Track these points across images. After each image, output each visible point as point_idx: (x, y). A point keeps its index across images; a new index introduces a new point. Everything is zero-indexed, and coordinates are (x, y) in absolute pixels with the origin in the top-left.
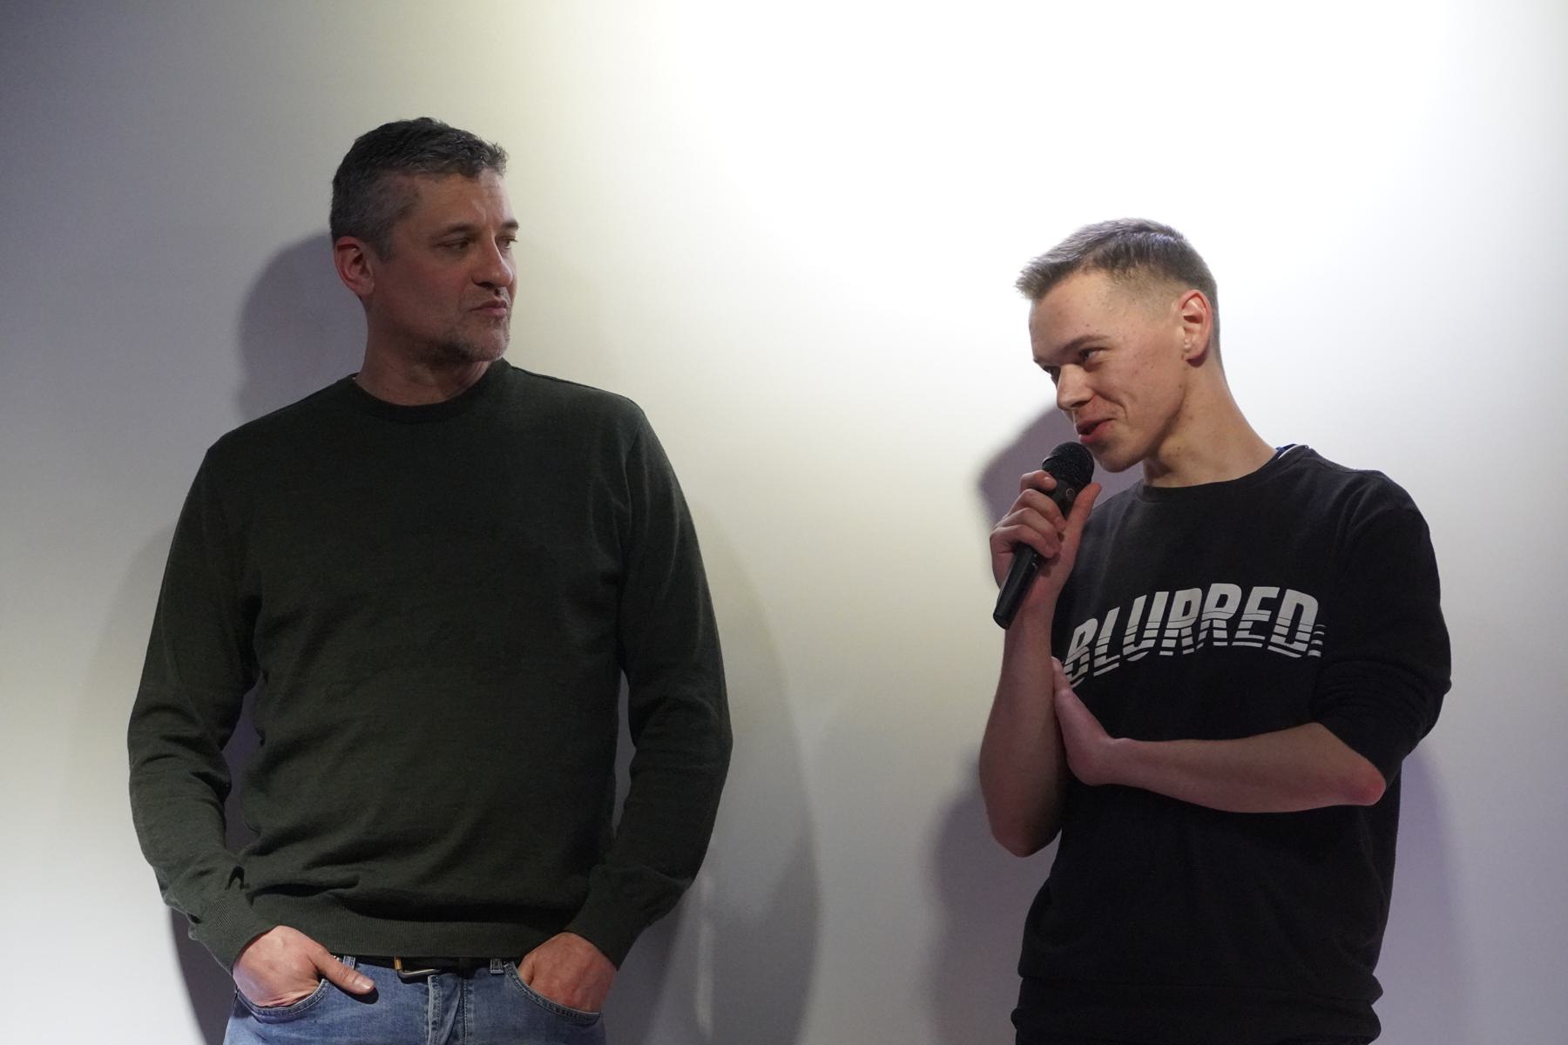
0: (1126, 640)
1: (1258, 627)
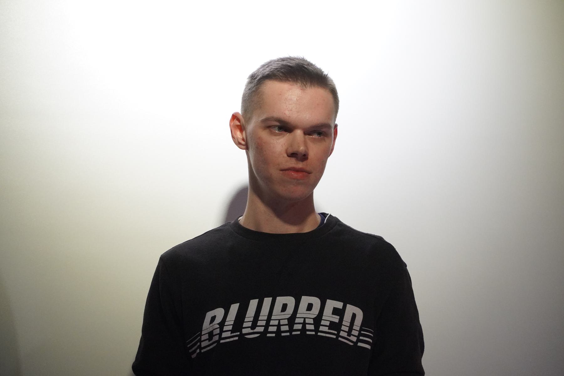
0: (245, 325)
1: (332, 326)
